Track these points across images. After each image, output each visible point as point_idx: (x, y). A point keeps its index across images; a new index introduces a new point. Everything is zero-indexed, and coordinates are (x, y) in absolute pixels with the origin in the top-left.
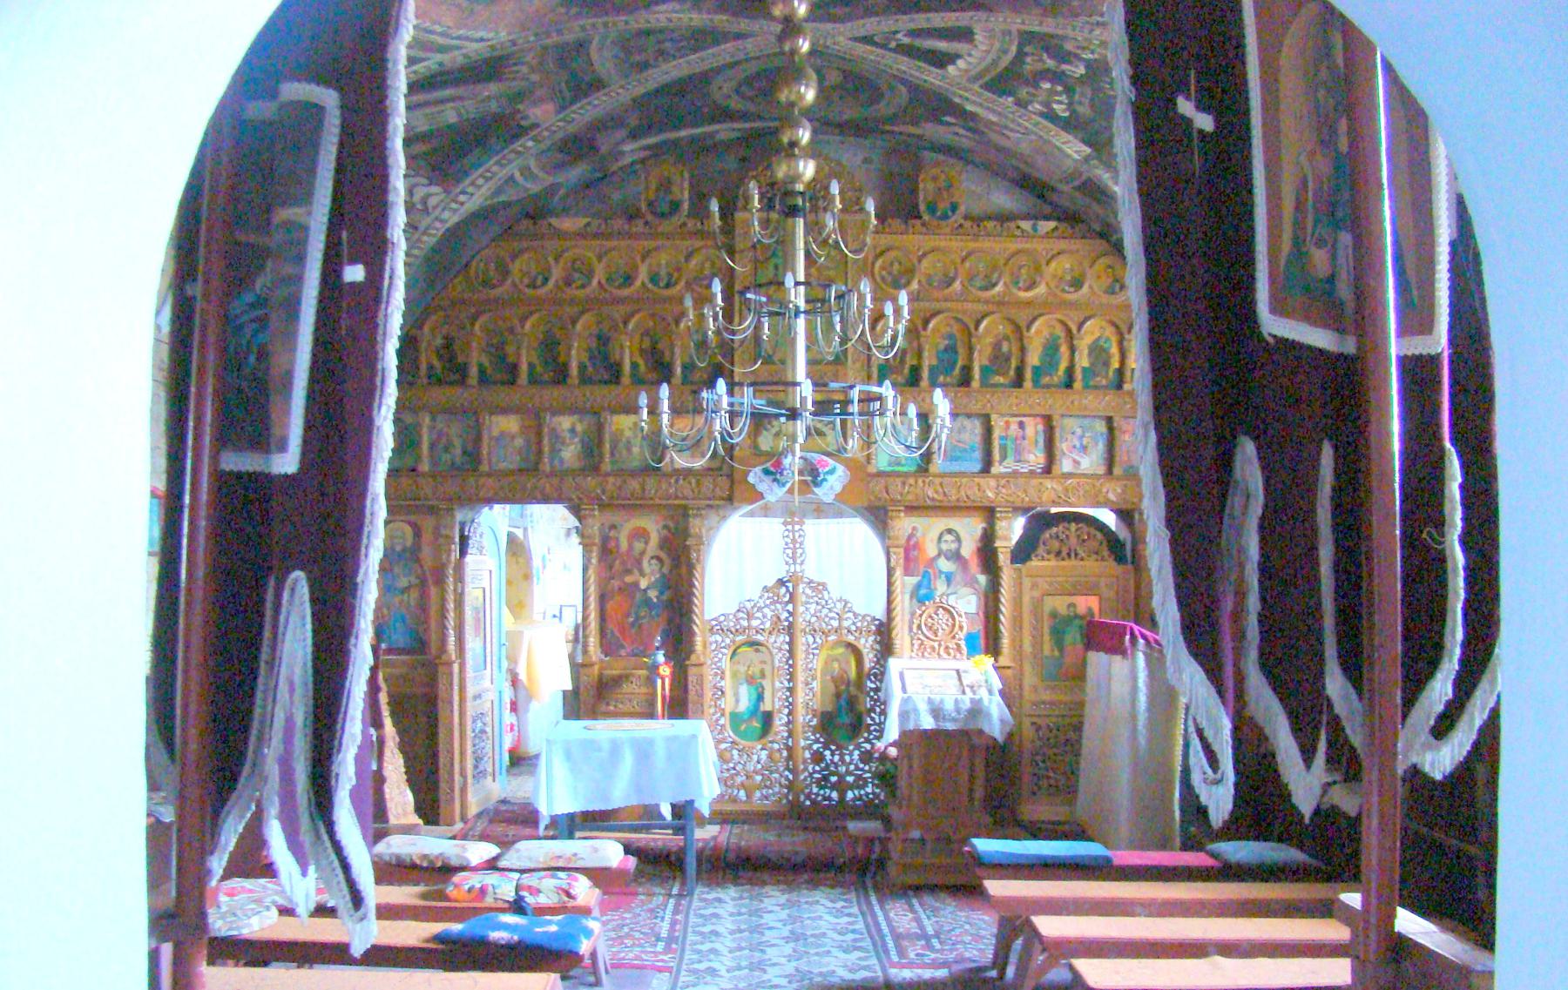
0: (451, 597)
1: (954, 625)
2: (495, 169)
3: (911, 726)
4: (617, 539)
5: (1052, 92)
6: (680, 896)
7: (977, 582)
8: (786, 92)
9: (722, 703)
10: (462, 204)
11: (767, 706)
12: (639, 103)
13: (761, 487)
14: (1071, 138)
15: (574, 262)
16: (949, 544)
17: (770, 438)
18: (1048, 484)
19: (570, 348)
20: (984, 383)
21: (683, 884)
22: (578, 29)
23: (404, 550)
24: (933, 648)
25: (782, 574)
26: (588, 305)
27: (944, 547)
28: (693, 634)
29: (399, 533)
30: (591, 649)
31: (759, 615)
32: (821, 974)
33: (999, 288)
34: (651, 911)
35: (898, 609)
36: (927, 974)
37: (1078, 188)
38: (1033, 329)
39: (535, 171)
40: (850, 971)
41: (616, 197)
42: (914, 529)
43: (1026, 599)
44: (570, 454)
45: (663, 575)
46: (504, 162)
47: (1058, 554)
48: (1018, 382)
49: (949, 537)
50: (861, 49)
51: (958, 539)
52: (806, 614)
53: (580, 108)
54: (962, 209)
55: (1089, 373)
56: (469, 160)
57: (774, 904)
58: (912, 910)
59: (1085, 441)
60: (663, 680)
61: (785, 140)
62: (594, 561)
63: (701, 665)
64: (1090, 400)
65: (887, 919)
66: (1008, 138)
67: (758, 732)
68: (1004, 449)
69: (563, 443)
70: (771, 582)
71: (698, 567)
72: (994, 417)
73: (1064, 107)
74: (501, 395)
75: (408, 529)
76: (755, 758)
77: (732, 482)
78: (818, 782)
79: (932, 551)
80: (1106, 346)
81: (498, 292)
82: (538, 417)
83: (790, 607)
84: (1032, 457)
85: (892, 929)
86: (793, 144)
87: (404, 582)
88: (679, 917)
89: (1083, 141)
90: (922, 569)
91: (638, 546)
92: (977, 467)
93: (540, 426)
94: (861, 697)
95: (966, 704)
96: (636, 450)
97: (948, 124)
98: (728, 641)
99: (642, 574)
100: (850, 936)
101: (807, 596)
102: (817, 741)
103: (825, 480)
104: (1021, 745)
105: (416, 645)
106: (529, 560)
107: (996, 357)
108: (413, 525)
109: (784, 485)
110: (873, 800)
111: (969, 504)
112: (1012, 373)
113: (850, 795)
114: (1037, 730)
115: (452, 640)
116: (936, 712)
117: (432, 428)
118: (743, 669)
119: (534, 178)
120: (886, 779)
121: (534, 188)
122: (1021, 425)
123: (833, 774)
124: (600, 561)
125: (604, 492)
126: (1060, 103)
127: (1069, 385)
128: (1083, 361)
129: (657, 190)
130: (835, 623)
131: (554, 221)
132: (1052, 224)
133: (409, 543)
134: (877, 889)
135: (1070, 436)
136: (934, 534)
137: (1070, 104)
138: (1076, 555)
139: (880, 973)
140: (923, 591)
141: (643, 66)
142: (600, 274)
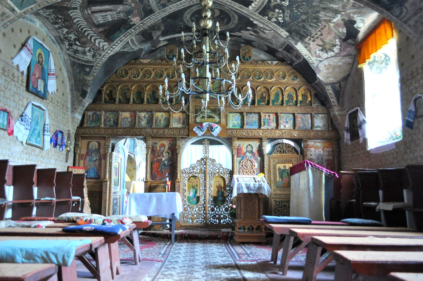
0: (108, 163)
2: (123, 38)
3: (241, 192)
4: (156, 147)
6: (170, 244)
7: (257, 159)
8: (204, 2)
9: (185, 194)
10: (114, 48)
11: (198, 195)
12: (164, 20)
13: (197, 132)
14: (283, 30)
15: (146, 71)
16: (249, 148)
17: (199, 119)
18: (277, 131)
19: (144, 94)
21: (171, 242)
23: (95, 149)
24: (246, 172)
25: (202, 157)
26: (149, 83)
27: (248, 149)
28: (177, 173)
29: (94, 145)
30: (148, 177)
31: (196, 168)
32: (213, 262)
33: (262, 79)
34: (159, 248)
35: (235, 169)
36: (250, 263)
37: (284, 49)
38: (272, 90)
39: (135, 42)
40: (223, 262)
41: (159, 55)
43: (271, 165)
44: (144, 123)
45: (169, 157)
47: (280, 152)
48: (268, 104)
49: (249, 147)
51: (252, 147)
52: (209, 168)
53: (147, 19)
54: (252, 58)
55: (288, 102)
56: (116, 34)
57: (199, 247)
58: (242, 248)
59: (287, 120)
60: (168, 185)
61: (203, 15)
62: (150, 153)
63: (179, 182)
64: (289, 109)
67: (196, 202)
68: (264, 122)
69: (142, 120)
70: (199, 159)
71: (179, 155)
72: (261, 113)
73: (282, 18)
74: (125, 106)
75: (97, 143)
76: (194, 210)
77: (189, 131)
78: (213, 217)
79: (245, 150)
80: (292, 94)
81: (124, 79)
82: (135, 112)
83: (205, 166)
85: (237, 253)
86: (206, 17)
87: (95, 159)
88: (168, 249)
89: (286, 31)
90: (242, 155)
91: (162, 149)
92: (257, 127)
93: (135, 115)
94: (225, 192)
95: (257, 186)
96: (162, 122)
97: (248, 30)
98: (187, 176)
99: (163, 157)
100: (223, 254)
102: (212, 205)
104: (271, 207)
105: (97, 177)
106: (135, 164)
107: (262, 98)
110: (228, 223)
111: (255, 137)
112: (266, 102)
113: (222, 221)
114: (276, 203)
115: (107, 175)
116: (248, 188)
117: (105, 116)
118: (191, 184)
119: (135, 45)
120: (233, 215)
121: (136, 49)
122: (269, 116)
123: (217, 214)
124: (151, 152)
125: (153, 133)
126: (281, 17)
127: (282, 104)
130: (218, 171)
131: (141, 60)
132: (277, 62)
133: (97, 147)
134: (231, 244)
135: (283, 119)
136: (245, 146)
137: (283, 18)
138: (285, 152)
139: (233, 262)
141: (164, 6)
142: (153, 75)
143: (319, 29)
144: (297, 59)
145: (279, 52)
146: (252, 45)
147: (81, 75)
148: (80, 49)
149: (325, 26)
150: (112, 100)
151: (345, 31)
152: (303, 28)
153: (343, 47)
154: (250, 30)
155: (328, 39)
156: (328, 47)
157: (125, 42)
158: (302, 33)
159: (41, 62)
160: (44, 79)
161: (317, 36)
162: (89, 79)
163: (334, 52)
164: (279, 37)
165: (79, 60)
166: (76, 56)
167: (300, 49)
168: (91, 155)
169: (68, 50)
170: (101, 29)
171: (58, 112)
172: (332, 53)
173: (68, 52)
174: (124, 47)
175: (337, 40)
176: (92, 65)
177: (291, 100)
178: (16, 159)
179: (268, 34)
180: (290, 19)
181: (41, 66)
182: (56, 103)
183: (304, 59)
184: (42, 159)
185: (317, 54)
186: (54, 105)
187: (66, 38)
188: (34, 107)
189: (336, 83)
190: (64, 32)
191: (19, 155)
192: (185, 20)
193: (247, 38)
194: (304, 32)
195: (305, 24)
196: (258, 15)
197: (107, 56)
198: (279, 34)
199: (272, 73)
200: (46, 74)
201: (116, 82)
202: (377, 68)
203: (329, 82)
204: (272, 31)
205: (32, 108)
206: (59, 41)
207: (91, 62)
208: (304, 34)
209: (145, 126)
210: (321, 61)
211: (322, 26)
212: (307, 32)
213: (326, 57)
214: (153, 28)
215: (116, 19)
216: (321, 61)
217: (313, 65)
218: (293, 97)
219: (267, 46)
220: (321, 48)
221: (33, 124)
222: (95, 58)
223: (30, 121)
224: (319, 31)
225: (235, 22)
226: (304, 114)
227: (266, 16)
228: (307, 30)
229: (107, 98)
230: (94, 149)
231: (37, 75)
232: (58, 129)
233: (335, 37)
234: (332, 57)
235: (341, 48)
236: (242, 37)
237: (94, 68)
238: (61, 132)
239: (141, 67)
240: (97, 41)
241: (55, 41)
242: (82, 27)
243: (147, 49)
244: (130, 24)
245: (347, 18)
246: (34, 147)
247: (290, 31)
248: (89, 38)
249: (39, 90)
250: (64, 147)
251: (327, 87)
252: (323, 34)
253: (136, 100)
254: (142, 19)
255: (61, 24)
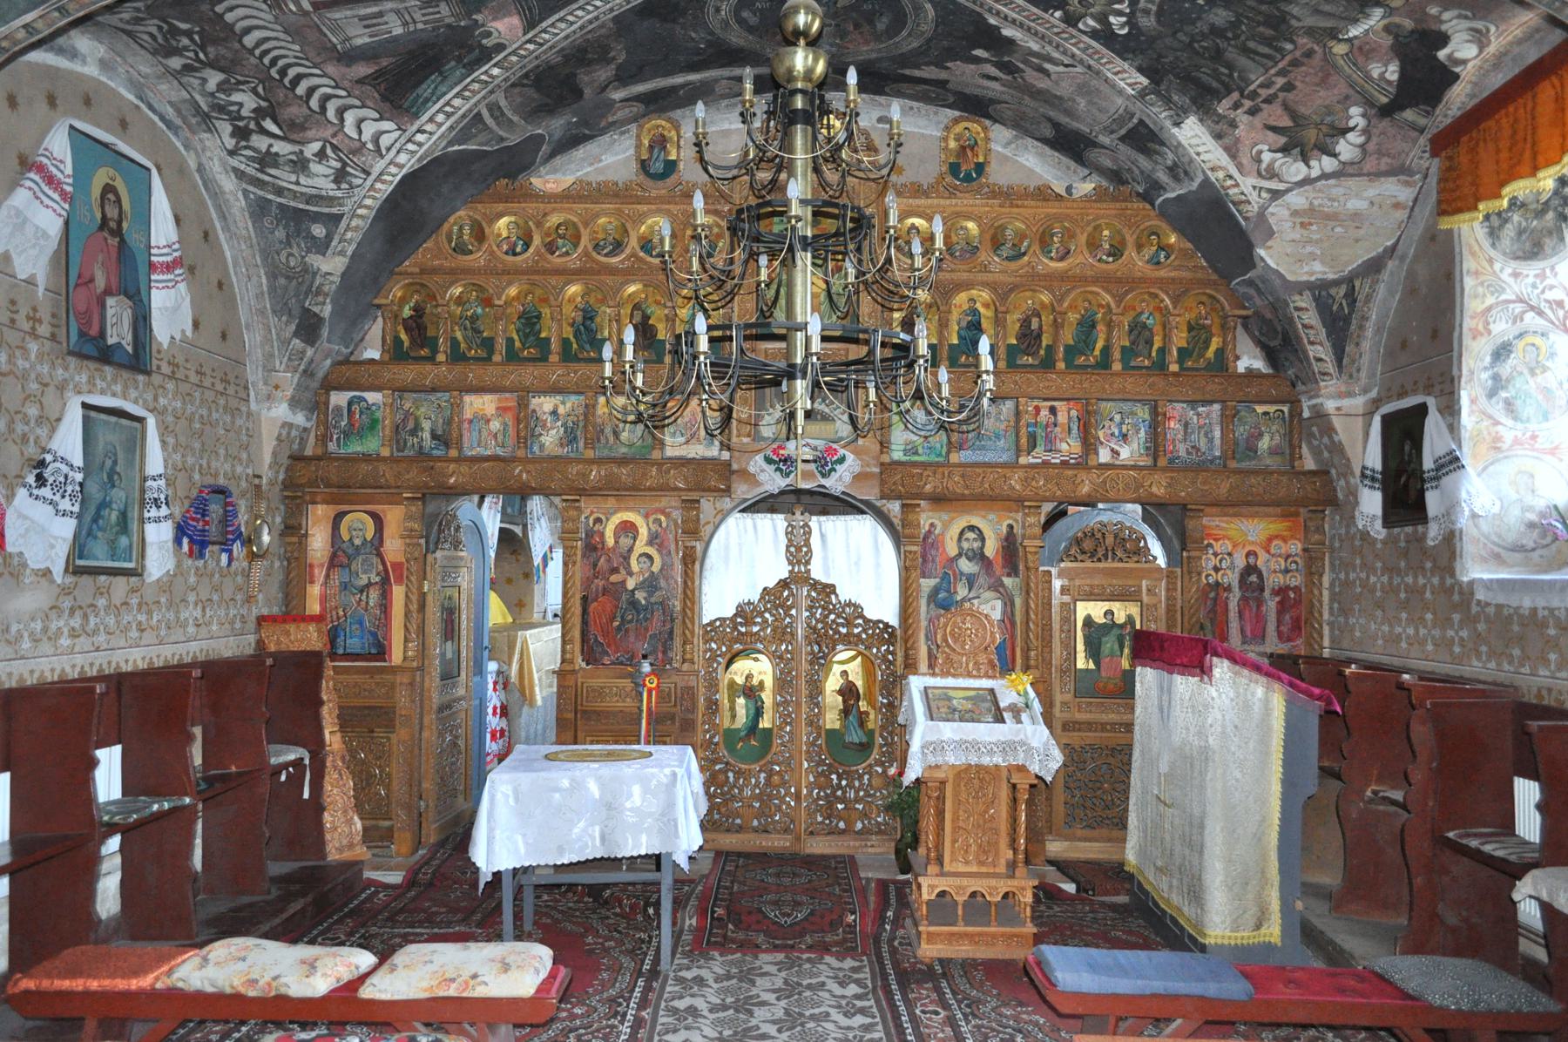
2: (457, 102)
4: (602, 535)
7: (1002, 585)
14: (1126, 66)
37: (1122, 139)
39: (509, 114)
42: (932, 525)
46: (467, 93)
49: (971, 535)
53: (553, 25)
56: (425, 89)
65: (914, 1020)
66: (1047, 73)
69: (544, 426)
74: (473, 374)
79: (952, 550)
84: (1064, 446)
87: (363, 580)
89: (1140, 70)
91: (625, 541)
107: (1025, 336)
108: (374, 516)
109: (788, 475)
112: (1042, 352)
121: (513, 139)
122: (1053, 410)
124: (584, 556)
126: (1120, 13)
128: (1121, 340)
129: (651, 147)
133: (369, 536)
135: (1107, 423)
140: (942, 595)
143: (1280, 65)
144: (1176, 178)
145: (1103, 147)
146: (988, 116)
147: (295, 251)
148: (280, 147)
149: (1309, 54)
150: (422, 347)
151: (1392, 72)
152: (1212, 58)
153: (1375, 139)
154: (986, 61)
155: (1313, 100)
156: (1311, 135)
157: (464, 116)
158: (1205, 78)
159: (113, 225)
160: (132, 291)
161: (1271, 91)
162: (325, 268)
163: (1335, 155)
164: (1104, 88)
165: (280, 191)
166: (267, 178)
167: (1194, 141)
168: (349, 566)
169: (232, 153)
170: (363, 70)
171: (204, 412)
172: (1326, 160)
173: (234, 162)
174: (463, 135)
175: (1355, 111)
176: (335, 210)
178: (26, 644)
179: (1062, 82)
180: (1158, 21)
181: (114, 241)
182: (194, 378)
183: (1206, 182)
184: (142, 618)
185: (1264, 166)
186: (184, 387)
187: (221, 109)
188: (93, 414)
189: (1336, 283)
190: (212, 85)
191: (38, 626)
192: (714, 22)
193: (967, 91)
194: (1216, 75)
195: (1222, 44)
197: (395, 176)
198: (1106, 80)
199: (1069, 235)
200: (142, 269)
201: (434, 271)
202: (1520, 233)
203: (1305, 278)
204: (1079, 69)
205: (86, 420)
206: (194, 121)
207: (331, 200)
208: (1215, 84)
209: (559, 451)
210: (1276, 195)
211: (1298, 54)
212: (1230, 76)
213: (1300, 177)
214: (583, 54)
215: (420, 26)
216: (1276, 195)
217: (1244, 208)
218: (1151, 330)
219: (1050, 120)
220: (1282, 140)
221: (93, 488)
222: (344, 186)
223: (79, 477)
224: (1282, 73)
225: (924, 27)
226: (1193, 403)
227: (1056, 9)
228: (1231, 67)
229: (403, 336)
230: (357, 542)
231: (100, 282)
232: (209, 480)
233: (1347, 97)
234: (1325, 176)
235: (1368, 140)
236: (950, 86)
237: (343, 224)
238: (221, 491)
239: (531, 207)
240: (350, 118)
241: (179, 122)
242: (281, 63)
243: (557, 136)
244: (480, 45)
245: (1408, 24)
246: (103, 578)
247: (1157, 71)
248: (314, 103)
249: (110, 341)
250: (237, 547)
251: (1297, 297)
252: (1297, 84)
253: (517, 344)
254: (530, 25)
255: (191, 54)
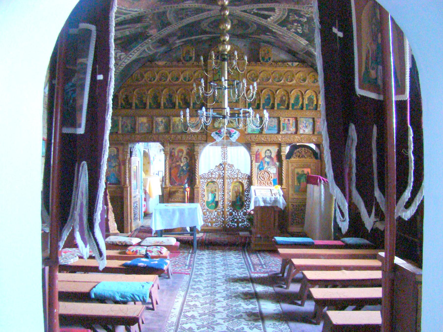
0: (127, 169)
1: (269, 177)
2: (140, 48)
3: (257, 205)
4: (174, 152)
5: (297, 26)
6: (192, 253)
7: (276, 164)
8: (222, 26)
9: (204, 199)
10: (131, 58)
11: (217, 199)
12: (181, 29)
13: (215, 138)
14: (303, 39)
15: (162, 74)
16: (268, 154)
17: (218, 124)
18: (296, 137)
19: (161, 98)
20: (278, 108)
21: (193, 250)
22: (163, 8)
23: (114, 155)
24: (264, 183)
25: (221, 162)
26: (166, 86)
27: (267, 154)
28: (195, 179)
29: (113, 151)
30: (167, 183)
31: (214, 174)
32: (232, 275)
33: (282, 81)
35: (254, 172)
37: (305, 53)
38: (292, 93)
39: (151, 48)
40: (240, 274)
41: (174, 55)
42: (258, 149)
43: (290, 169)
44: (161, 128)
45: (187, 162)
46: (142, 46)
47: (299, 156)
48: (288, 108)
49: (268, 152)
50: (243, 14)
51: (271, 152)
52: (228, 173)
53: (164, 31)
54: (272, 59)
55: (308, 105)
57: (219, 255)
59: (306, 125)
60: (187, 192)
61: (222, 39)
62: (168, 158)
63: (198, 188)
65: (251, 260)
66: (285, 39)
67: (214, 207)
68: (284, 127)
69: (159, 125)
70: (218, 165)
71: (197, 160)
72: (281, 118)
73: (301, 30)
74: (142, 112)
75: (115, 150)
76: (213, 214)
77: (207, 136)
78: (231, 221)
79: (263, 155)
80: (312, 98)
81: (141, 82)
82: (152, 118)
83: (223, 171)
84: (291, 129)
85: (252, 263)
86: (224, 41)
87: (114, 164)
89: (306, 40)
90: (260, 161)
91: (180, 154)
92: (276, 132)
93: (152, 120)
94: (243, 197)
95: (273, 199)
96: (180, 127)
97: (268, 35)
98: (206, 181)
99: (182, 162)
100: (240, 265)
101: (228, 168)
102: (231, 209)
103: (233, 136)
104: (288, 211)
106: (149, 158)
108: (116, 148)
109: (221, 137)
110: (247, 226)
111: (274, 142)
112: (286, 105)
113: (240, 225)
114: (293, 206)
115: (128, 181)
116: (265, 201)
117: (122, 121)
118: (210, 189)
120: (250, 220)
121: (151, 53)
122: (289, 120)
123: (235, 219)
124: (169, 158)
125: (170, 139)
126: (299, 29)
127: (302, 109)
128: (306, 102)
129: (186, 54)
130: (236, 176)
131: (157, 62)
132: (297, 63)
133: (116, 153)
134: (248, 251)
135: (302, 123)
136: (264, 151)
137: (302, 29)
138: (304, 157)
139: (249, 275)
140: (261, 167)
141: (182, 19)
142: (169, 77)
177: (311, 104)
196: (277, 25)
214: (169, 36)
239: (156, 69)
